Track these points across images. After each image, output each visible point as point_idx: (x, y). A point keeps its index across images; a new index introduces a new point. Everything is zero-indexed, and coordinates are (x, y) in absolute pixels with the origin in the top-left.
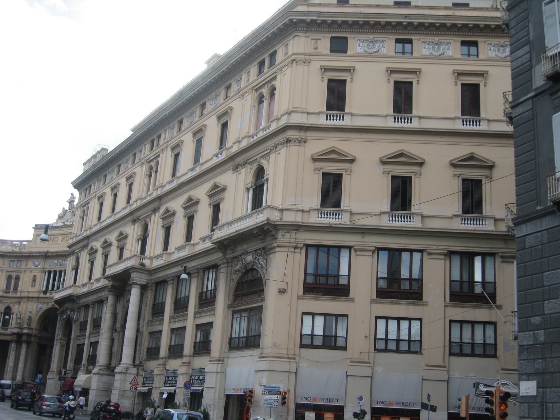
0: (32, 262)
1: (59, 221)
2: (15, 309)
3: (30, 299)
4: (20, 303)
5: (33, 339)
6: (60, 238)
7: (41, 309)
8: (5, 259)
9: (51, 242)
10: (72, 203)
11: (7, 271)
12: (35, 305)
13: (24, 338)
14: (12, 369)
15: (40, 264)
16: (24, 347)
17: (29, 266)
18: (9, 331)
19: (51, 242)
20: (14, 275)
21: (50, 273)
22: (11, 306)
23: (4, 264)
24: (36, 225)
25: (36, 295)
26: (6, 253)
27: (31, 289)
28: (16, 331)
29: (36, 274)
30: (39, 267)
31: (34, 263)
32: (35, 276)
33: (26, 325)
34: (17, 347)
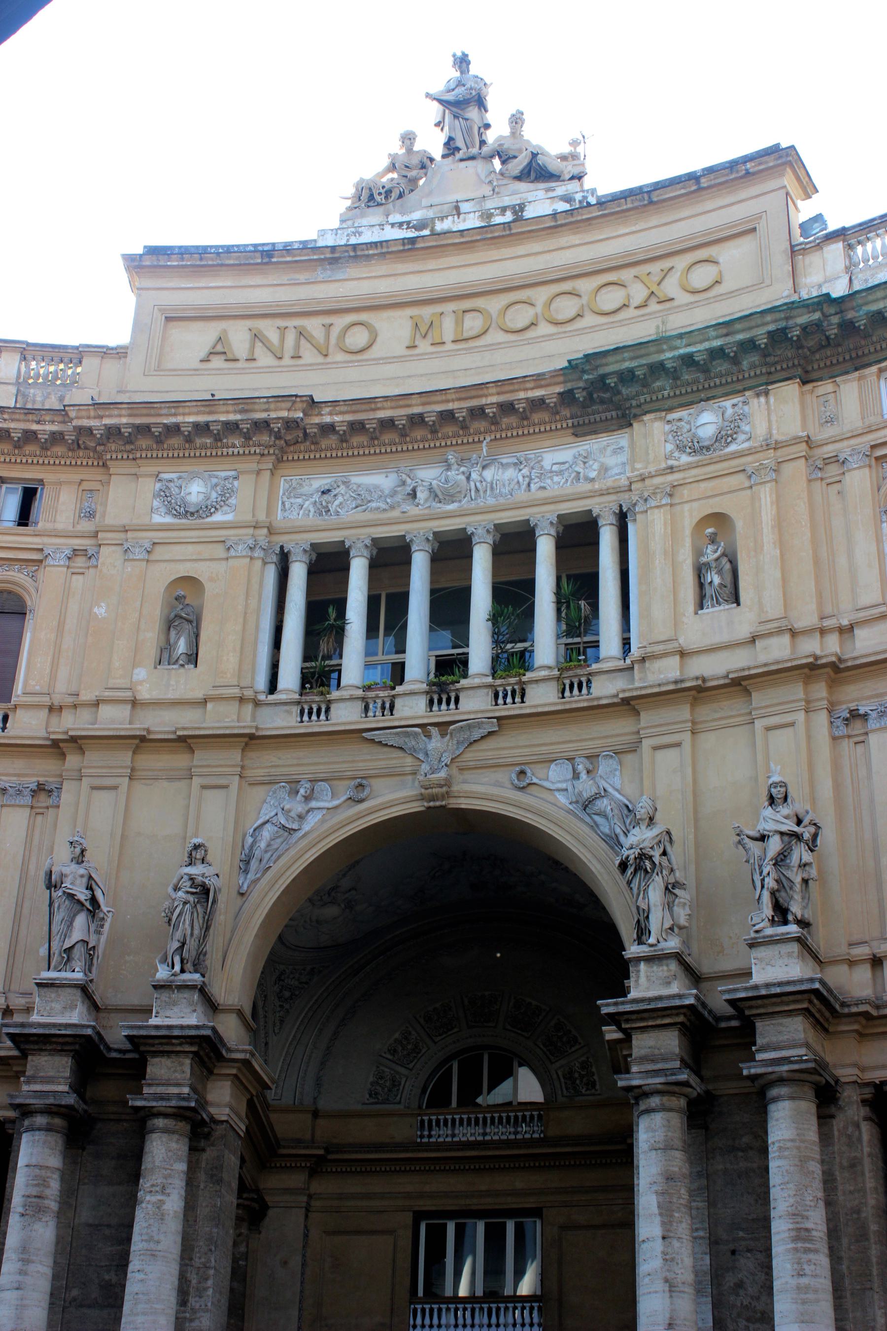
0: (149, 486)
1: (374, 217)
3: (149, 761)
13: (169, 1078)
27: (147, 681)
30: (218, 517)
31: (164, 495)
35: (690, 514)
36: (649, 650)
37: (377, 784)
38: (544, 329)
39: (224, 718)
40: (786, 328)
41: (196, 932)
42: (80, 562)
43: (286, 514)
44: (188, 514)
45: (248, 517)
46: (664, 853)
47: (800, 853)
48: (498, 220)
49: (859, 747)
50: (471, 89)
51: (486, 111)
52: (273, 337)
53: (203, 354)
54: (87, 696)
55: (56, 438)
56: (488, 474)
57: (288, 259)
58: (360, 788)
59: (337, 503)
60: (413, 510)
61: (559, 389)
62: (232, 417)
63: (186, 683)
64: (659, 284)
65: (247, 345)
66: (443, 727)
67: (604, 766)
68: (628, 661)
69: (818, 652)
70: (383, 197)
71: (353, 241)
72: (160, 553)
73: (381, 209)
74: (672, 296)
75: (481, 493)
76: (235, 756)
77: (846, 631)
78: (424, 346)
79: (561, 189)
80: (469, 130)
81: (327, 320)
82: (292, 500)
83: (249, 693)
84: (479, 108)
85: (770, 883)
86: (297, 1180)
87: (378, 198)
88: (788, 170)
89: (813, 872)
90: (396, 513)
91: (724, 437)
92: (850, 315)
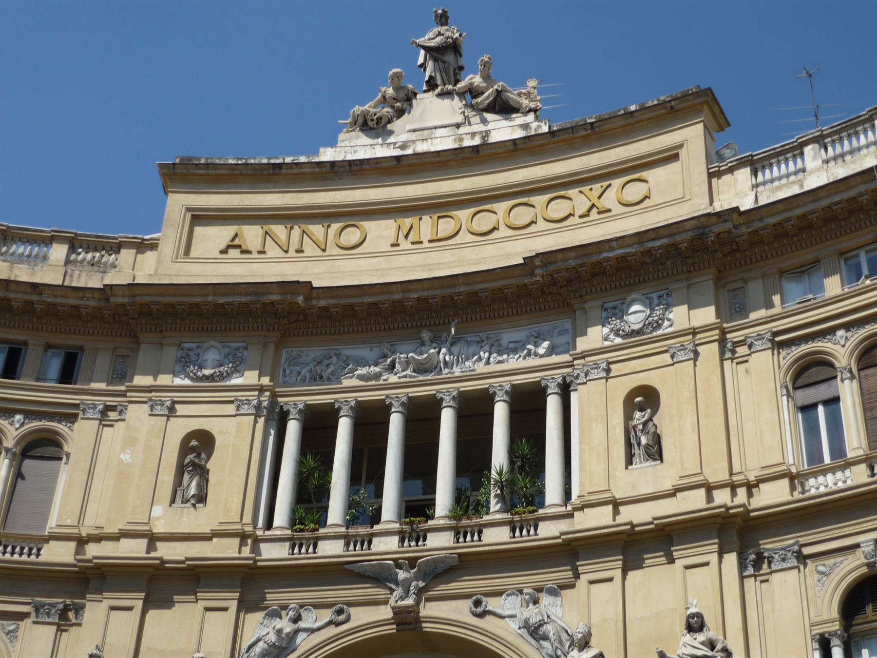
27: (164, 518)
35: (621, 387)
36: (586, 498)
38: (504, 232)
39: (226, 550)
40: (703, 234)
42: (112, 415)
43: (286, 379)
48: (468, 142)
49: (763, 585)
50: (447, 38)
51: (461, 56)
53: (222, 247)
57: (296, 171)
58: (341, 611)
59: (329, 371)
60: (393, 379)
64: (599, 197)
65: (260, 240)
66: (412, 562)
68: (569, 508)
69: (730, 504)
70: (375, 122)
71: (350, 157)
73: (373, 132)
74: (609, 207)
75: (450, 365)
77: (751, 487)
78: (405, 245)
79: (519, 119)
82: (292, 368)
84: (455, 54)
87: (370, 124)
88: (705, 107)
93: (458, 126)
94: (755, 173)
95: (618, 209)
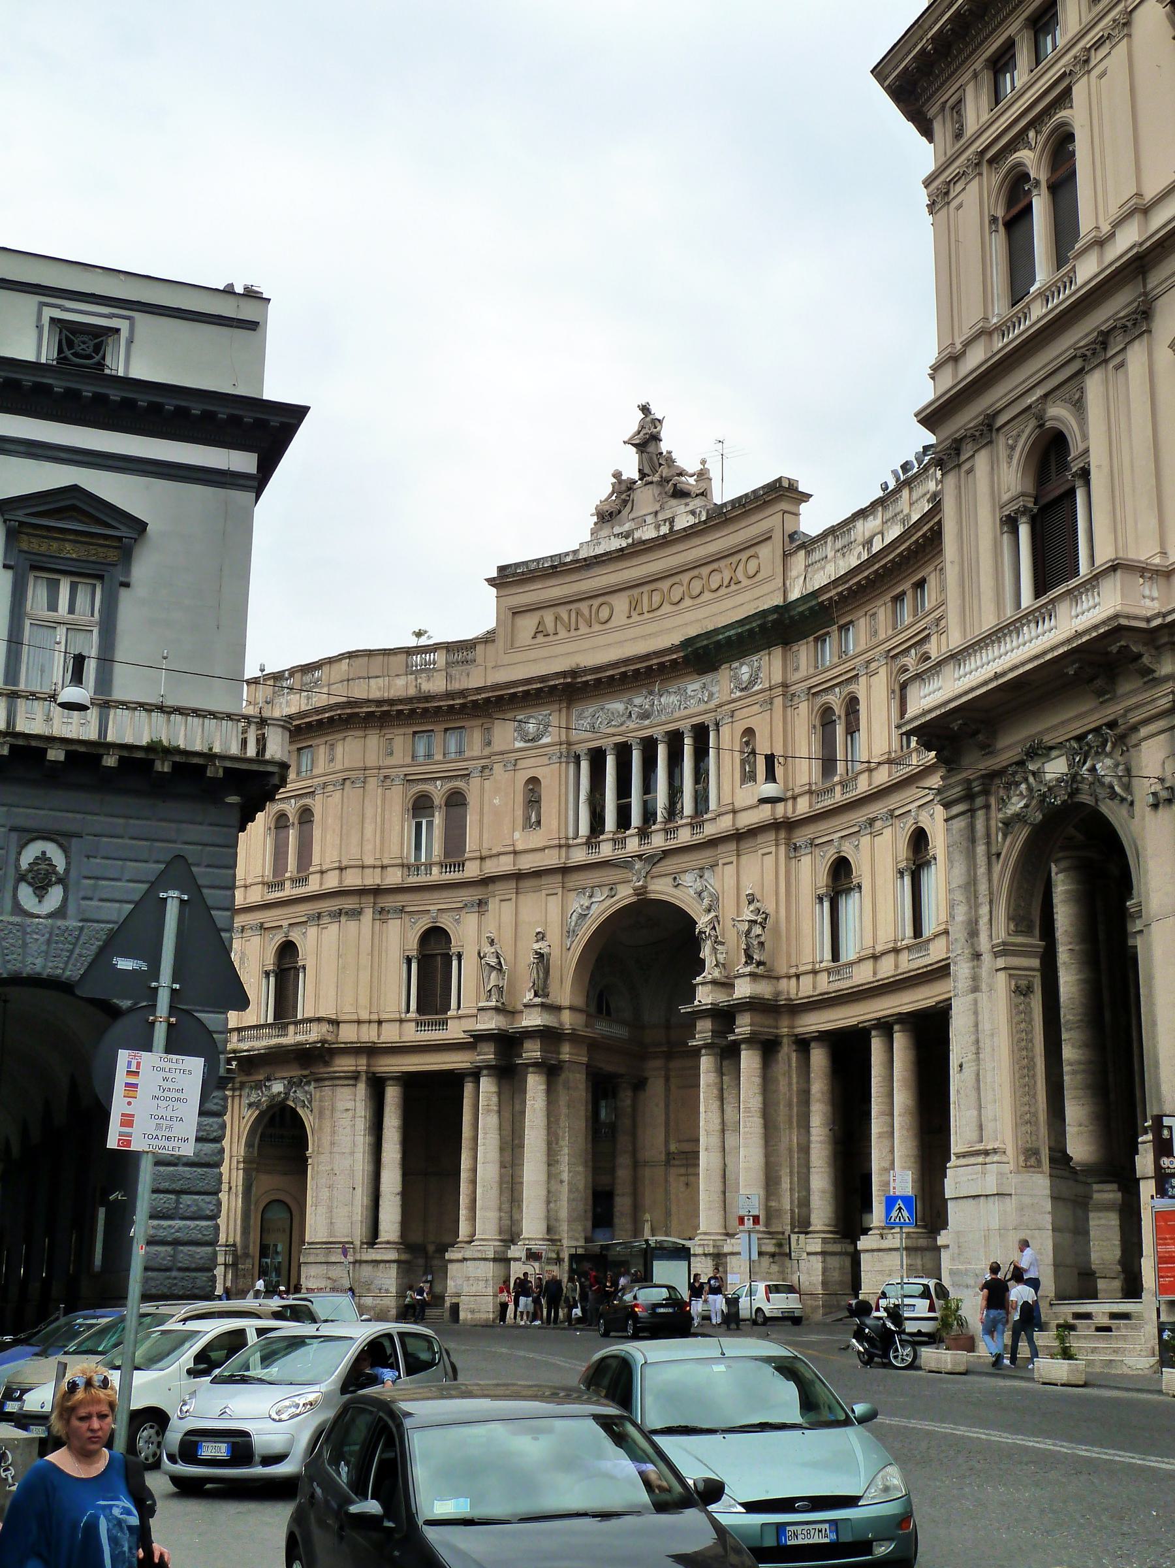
1: (605, 532)
2: (467, 934)
4: (481, 903)
5: (566, 1052)
6: (621, 603)
7: (583, 916)
8: (390, 733)
9: (583, 629)
10: (651, 448)
11: (408, 780)
12: (554, 904)
13: (532, 1051)
14: (494, 1193)
15: (550, 726)
16: (535, 1085)
17: (497, 746)
18: (455, 1031)
19: (583, 629)
20: (438, 792)
21: (597, 758)
22: (445, 922)
23: (391, 754)
24: (501, 569)
25: (551, 859)
26: (391, 702)
27: (522, 840)
28: (490, 1023)
29: (538, 773)
30: (546, 740)
31: (519, 730)
32: (534, 781)
33: (529, 996)
34: (499, 1094)
35: (740, 727)
37: (619, 887)
41: (541, 975)
44: (529, 741)
45: (557, 739)
46: (714, 928)
47: (757, 930)
52: (565, 616)
53: (532, 634)
54: (494, 852)
55: (463, 705)
56: (662, 700)
60: (632, 726)
61: (682, 654)
62: (539, 686)
63: (537, 839)
67: (707, 874)
72: (521, 764)
76: (559, 878)
80: (651, 459)
81: (590, 602)
83: (563, 842)
85: (744, 946)
86: (658, 1063)
89: (762, 939)
90: (623, 728)
91: (753, 681)
92: (793, 613)
93: (656, 513)
94: (808, 553)
95: (745, 582)
